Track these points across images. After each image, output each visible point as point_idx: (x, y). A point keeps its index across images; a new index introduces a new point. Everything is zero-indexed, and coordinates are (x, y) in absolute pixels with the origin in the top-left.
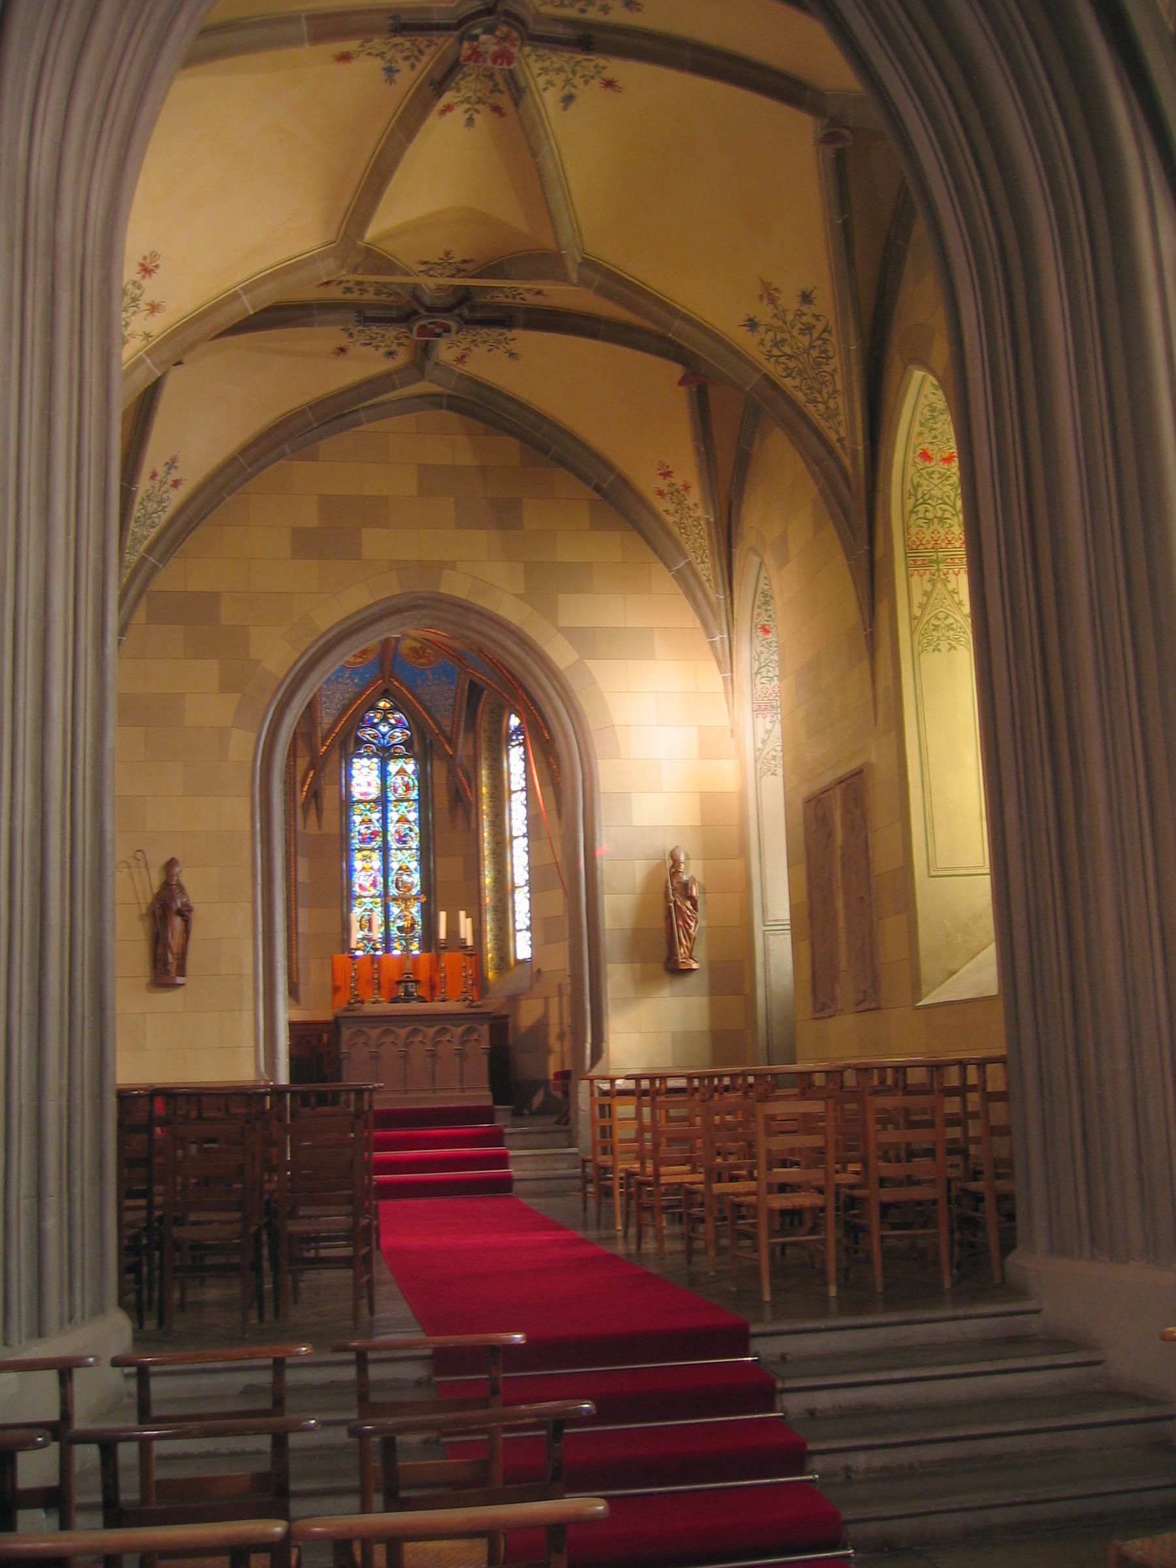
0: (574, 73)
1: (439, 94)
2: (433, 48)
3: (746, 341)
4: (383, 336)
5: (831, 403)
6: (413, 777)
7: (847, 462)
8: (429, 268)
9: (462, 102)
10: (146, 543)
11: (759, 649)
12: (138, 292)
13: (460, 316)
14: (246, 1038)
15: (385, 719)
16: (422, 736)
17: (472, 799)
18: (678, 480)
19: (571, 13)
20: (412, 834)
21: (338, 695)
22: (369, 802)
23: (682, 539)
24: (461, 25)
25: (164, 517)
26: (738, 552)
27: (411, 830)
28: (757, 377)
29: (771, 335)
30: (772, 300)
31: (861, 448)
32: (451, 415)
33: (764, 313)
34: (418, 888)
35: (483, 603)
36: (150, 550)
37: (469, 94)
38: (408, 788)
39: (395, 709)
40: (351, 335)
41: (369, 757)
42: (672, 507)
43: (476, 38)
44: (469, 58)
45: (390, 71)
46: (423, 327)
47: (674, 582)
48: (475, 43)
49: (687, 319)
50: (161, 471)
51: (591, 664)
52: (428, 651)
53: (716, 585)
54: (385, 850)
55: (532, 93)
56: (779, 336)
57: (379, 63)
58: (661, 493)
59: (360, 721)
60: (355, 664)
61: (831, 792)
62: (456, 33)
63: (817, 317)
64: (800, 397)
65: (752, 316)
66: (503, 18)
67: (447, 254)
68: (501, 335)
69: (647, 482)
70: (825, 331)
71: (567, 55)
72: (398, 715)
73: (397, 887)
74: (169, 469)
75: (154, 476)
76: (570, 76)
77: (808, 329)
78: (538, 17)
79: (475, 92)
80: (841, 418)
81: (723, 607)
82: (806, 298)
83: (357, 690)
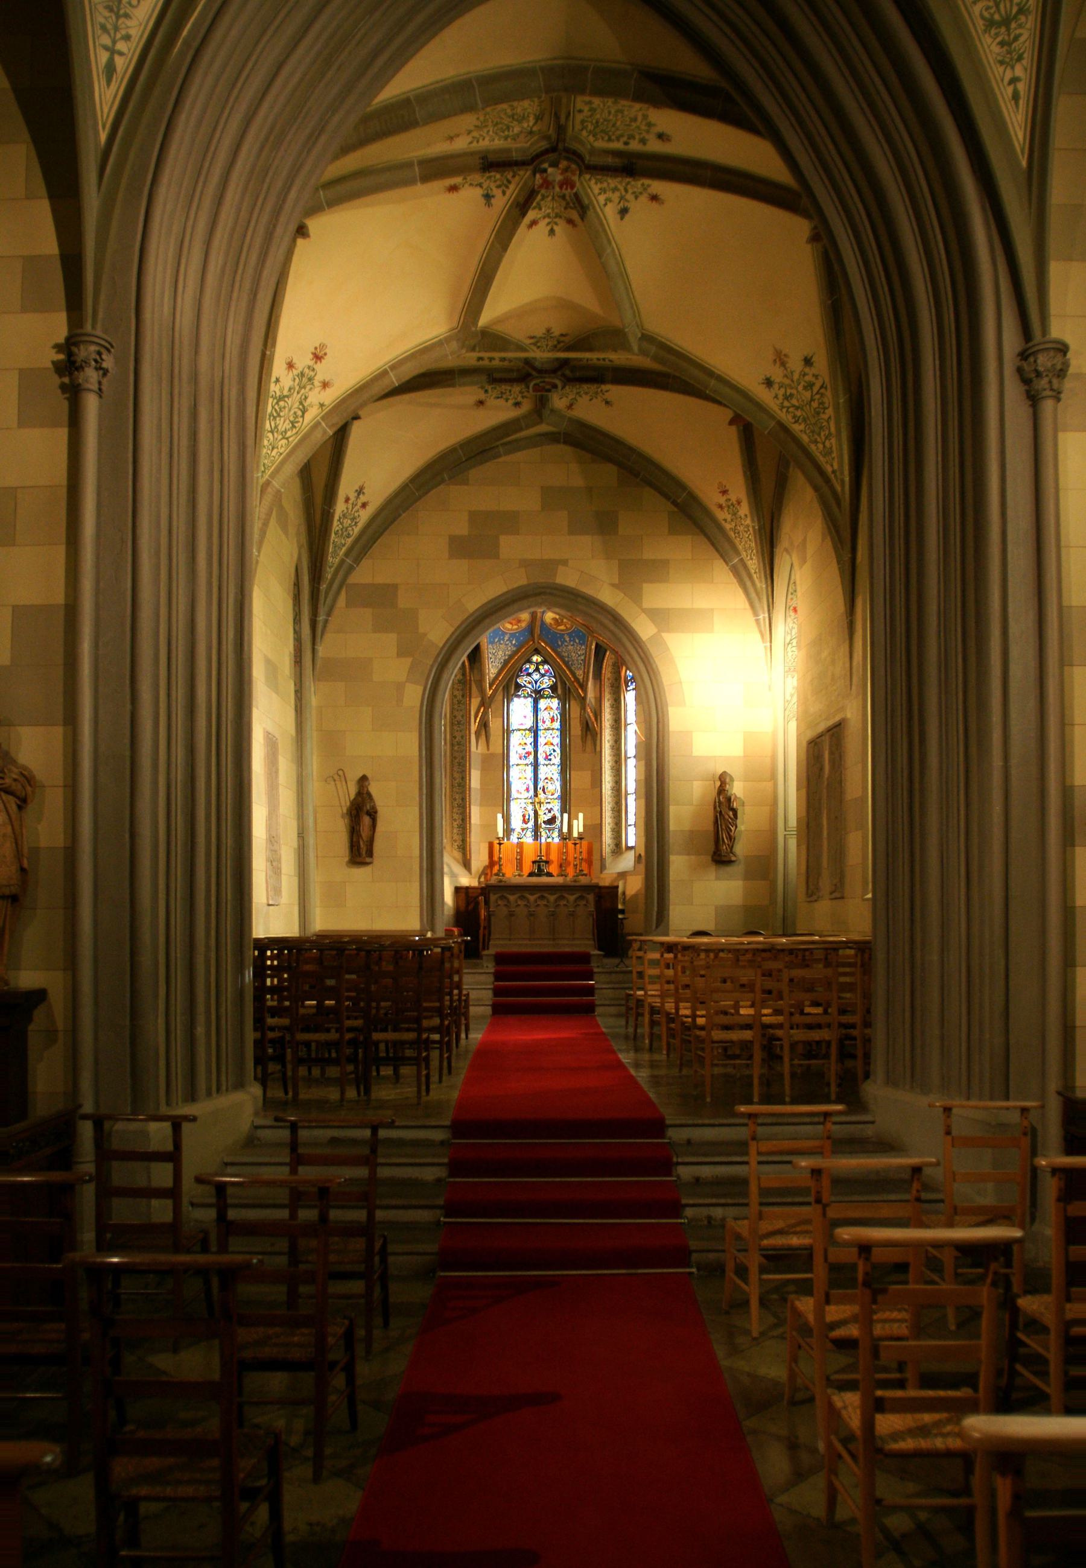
0: (626, 191)
1: (524, 214)
2: (517, 178)
3: (765, 396)
4: (510, 391)
5: (827, 444)
6: (556, 712)
7: (838, 488)
8: (536, 341)
9: (544, 218)
10: (344, 549)
11: (791, 625)
12: (312, 374)
13: (563, 375)
14: (415, 901)
15: (537, 670)
16: (564, 683)
17: (598, 729)
18: (733, 497)
19: (618, 145)
20: (555, 753)
21: (500, 653)
22: (525, 730)
23: (737, 541)
24: (533, 161)
25: (357, 530)
26: (778, 551)
27: (554, 751)
28: (772, 424)
29: (783, 390)
30: (783, 364)
31: (847, 479)
32: (567, 449)
33: (777, 375)
34: (559, 793)
35: (589, 591)
36: (347, 554)
37: (548, 211)
38: (553, 720)
39: (545, 662)
40: (486, 391)
41: (525, 697)
42: (729, 517)
43: (545, 171)
44: (541, 186)
45: (488, 197)
46: (535, 385)
47: (731, 574)
48: (545, 175)
49: (720, 378)
50: (352, 496)
51: (664, 635)
52: (565, 620)
53: (760, 577)
54: (536, 765)
55: (594, 207)
56: (789, 391)
57: (478, 192)
58: (721, 507)
59: (519, 671)
60: (511, 630)
61: (823, 738)
62: (531, 167)
63: (816, 377)
64: (805, 439)
65: (768, 376)
66: (564, 154)
67: (548, 330)
68: (598, 388)
69: (711, 497)
70: (822, 387)
71: (619, 179)
72: (546, 667)
73: (545, 793)
74: (359, 495)
75: (347, 500)
76: (624, 193)
77: (809, 386)
78: (593, 151)
79: (553, 209)
80: (834, 455)
81: (765, 591)
82: (808, 361)
83: (514, 649)
